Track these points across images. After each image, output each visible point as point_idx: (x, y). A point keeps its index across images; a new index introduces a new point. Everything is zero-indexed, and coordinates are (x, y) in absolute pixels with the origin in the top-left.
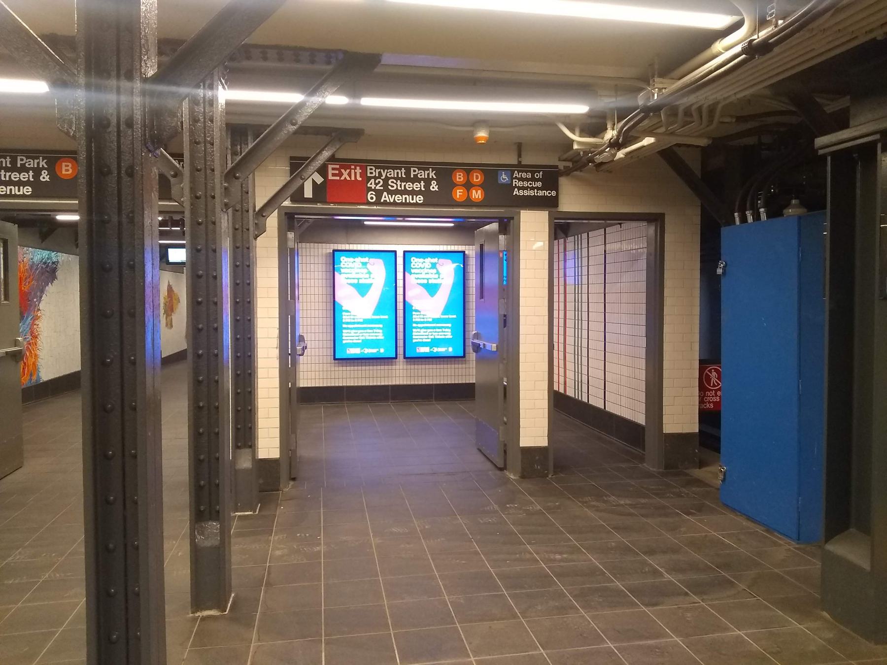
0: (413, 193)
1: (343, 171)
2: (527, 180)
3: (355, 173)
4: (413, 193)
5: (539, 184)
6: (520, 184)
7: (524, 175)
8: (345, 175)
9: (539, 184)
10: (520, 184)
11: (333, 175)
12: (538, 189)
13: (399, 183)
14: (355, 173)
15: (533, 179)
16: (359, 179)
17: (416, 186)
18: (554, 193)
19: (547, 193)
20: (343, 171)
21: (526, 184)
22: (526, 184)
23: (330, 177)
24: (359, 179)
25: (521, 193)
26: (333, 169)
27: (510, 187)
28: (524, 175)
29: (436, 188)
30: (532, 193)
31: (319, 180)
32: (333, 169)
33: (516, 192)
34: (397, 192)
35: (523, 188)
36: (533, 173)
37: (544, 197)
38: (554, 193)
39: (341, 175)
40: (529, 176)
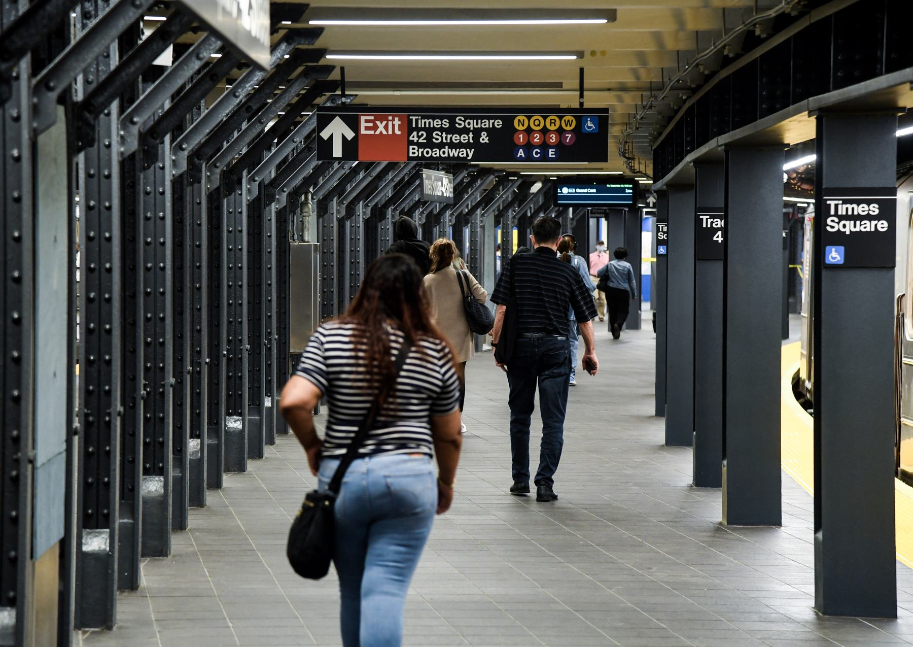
0: (460, 145)
1: (378, 123)
3: (393, 126)
8: (381, 127)
11: (367, 128)
14: (393, 126)
16: (398, 132)
17: (464, 138)
20: (378, 123)
23: (363, 131)
24: (398, 132)
29: (486, 140)
31: (350, 135)
32: (366, 121)
34: (441, 146)
39: (375, 128)
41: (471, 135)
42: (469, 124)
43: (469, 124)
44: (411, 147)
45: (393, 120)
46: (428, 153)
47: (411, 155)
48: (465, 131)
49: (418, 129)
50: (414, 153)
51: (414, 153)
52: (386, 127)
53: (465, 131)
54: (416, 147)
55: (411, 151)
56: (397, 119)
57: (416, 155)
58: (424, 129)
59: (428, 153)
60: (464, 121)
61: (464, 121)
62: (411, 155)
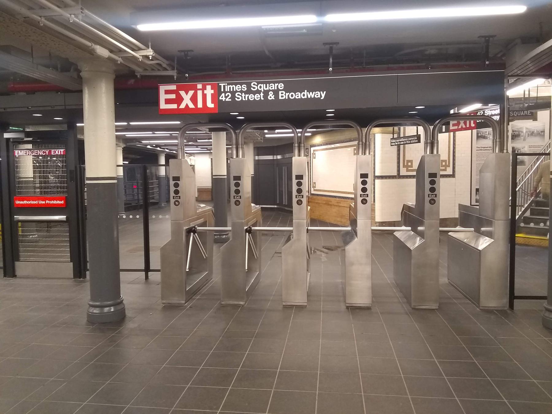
1: (182, 93)
13: (243, 95)
20: (182, 93)
41: (262, 94)
42: (261, 87)
43: (261, 87)
44: (280, 92)
45: (204, 88)
46: (292, 96)
47: (280, 98)
48: (258, 92)
49: (225, 92)
50: (282, 96)
51: (282, 96)
53: (258, 92)
54: (284, 92)
55: (280, 95)
56: (209, 87)
57: (284, 98)
58: (230, 92)
59: (292, 96)
60: (257, 86)
61: (257, 86)
62: (280, 98)
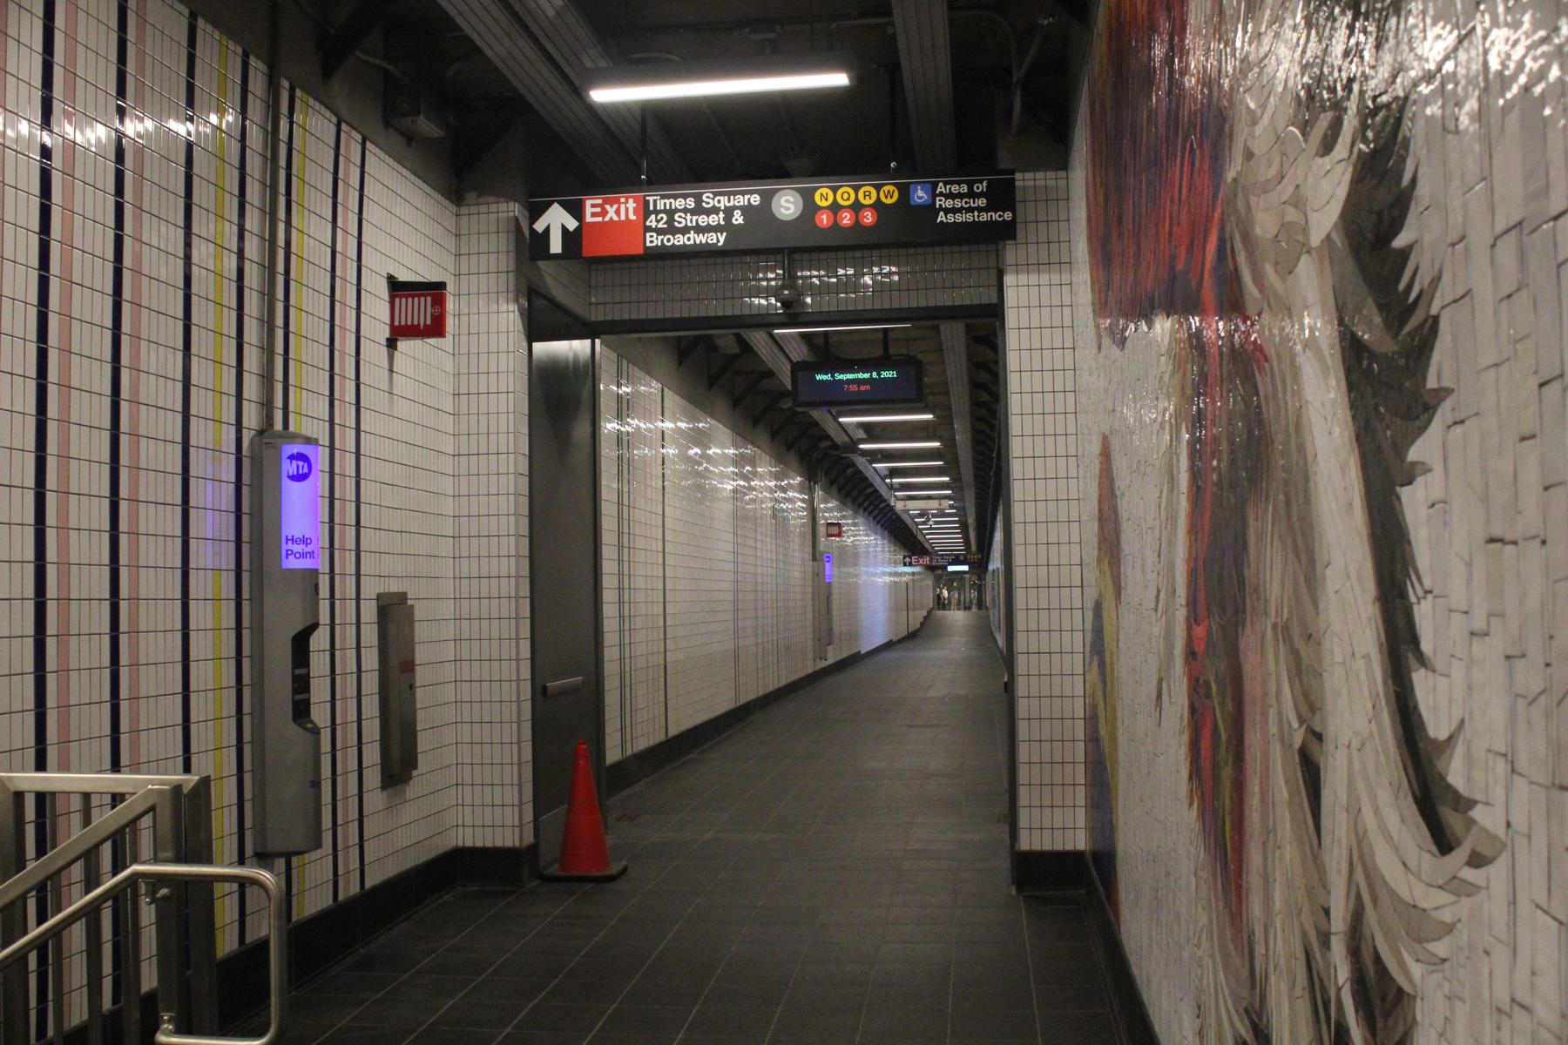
2: (960, 196)
4: (709, 229)
5: (982, 202)
6: (949, 204)
7: (955, 189)
9: (982, 202)
10: (949, 204)
11: (593, 215)
12: (980, 209)
15: (971, 194)
16: (632, 217)
18: (1008, 216)
19: (996, 216)
21: (958, 203)
22: (958, 203)
23: (589, 219)
24: (632, 217)
25: (951, 218)
26: (593, 206)
27: (930, 210)
28: (955, 189)
30: (969, 218)
31: (572, 224)
32: (593, 206)
33: (941, 217)
35: (954, 211)
36: (970, 184)
37: (991, 223)
38: (1008, 216)
39: (604, 213)
40: (964, 189)
52: (618, 212)
